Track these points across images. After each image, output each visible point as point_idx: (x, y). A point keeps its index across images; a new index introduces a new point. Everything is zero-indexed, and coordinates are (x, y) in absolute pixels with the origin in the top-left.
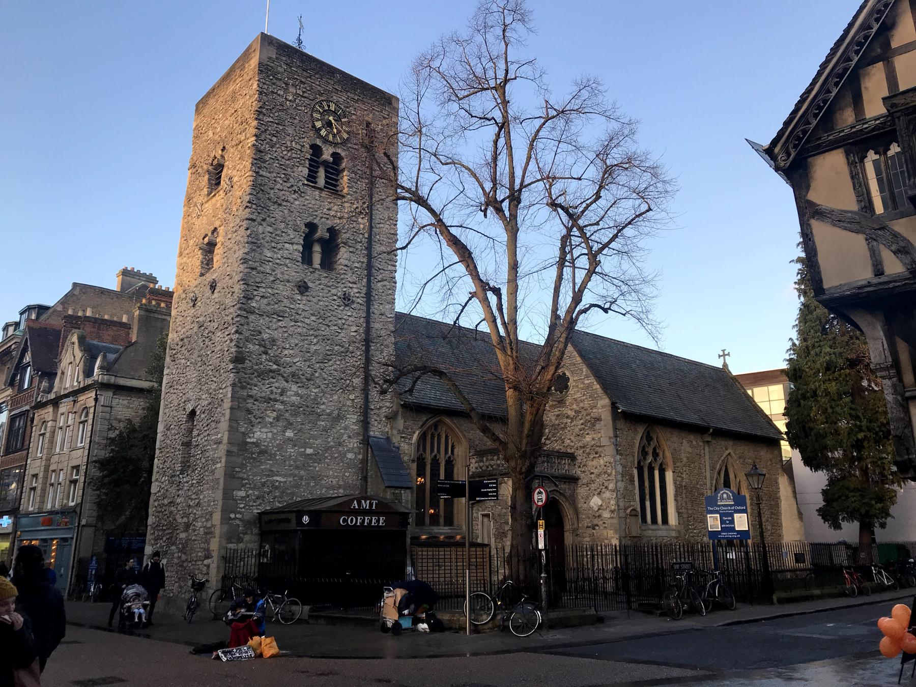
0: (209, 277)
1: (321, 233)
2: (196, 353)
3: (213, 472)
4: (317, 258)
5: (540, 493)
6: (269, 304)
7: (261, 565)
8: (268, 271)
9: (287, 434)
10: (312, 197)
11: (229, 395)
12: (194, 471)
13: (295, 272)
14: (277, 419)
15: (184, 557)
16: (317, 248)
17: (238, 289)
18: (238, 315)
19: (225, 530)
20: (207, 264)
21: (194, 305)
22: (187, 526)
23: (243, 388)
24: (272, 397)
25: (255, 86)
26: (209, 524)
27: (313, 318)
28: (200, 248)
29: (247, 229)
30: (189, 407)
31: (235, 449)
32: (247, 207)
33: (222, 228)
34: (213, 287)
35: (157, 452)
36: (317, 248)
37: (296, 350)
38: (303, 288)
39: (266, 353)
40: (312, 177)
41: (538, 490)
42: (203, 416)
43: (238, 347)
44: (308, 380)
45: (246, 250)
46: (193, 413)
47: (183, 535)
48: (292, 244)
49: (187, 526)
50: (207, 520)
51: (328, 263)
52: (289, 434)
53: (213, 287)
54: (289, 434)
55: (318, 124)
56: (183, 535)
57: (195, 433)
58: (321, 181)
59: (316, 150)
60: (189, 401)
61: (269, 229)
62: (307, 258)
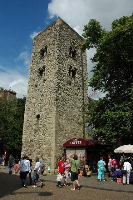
0: (42, 79)
4: (71, 75)
6: (62, 86)
8: (62, 76)
13: (68, 78)
18: (56, 87)
19: (56, 148)
26: (49, 147)
27: (72, 91)
28: (38, 72)
29: (57, 65)
30: (37, 114)
31: (57, 125)
32: (57, 59)
34: (44, 81)
35: (24, 127)
37: (69, 99)
38: (70, 83)
39: (63, 99)
40: (70, 54)
42: (43, 116)
43: (56, 96)
45: (58, 70)
46: (38, 116)
48: (67, 70)
51: (74, 76)
54: (68, 122)
55: (72, 42)
60: (37, 112)
61: (62, 65)
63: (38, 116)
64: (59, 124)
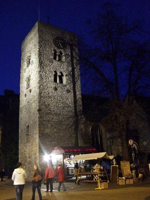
0: (29, 89)
1: (59, 74)
2: (28, 110)
3: (35, 142)
5: (131, 141)
7: (57, 168)
9: (55, 130)
10: (55, 63)
11: (38, 120)
12: (30, 142)
13: (53, 85)
14: (51, 126)
15: (29, 166)
16: (58, 78)
17: (38, 91)
20: (28, 85)
21: (26, 97)
22: (30, 157)
23: (41, 118)
24: (50, 120)
25: (38, 35)
30: (27, 125)
31: (41, 135)
33: (32, 75)
36: (58, 78)
40: (55, 58)
41: (130, 140)
44: (59, 115)
46: (28, 126)
47: (29, 160)
49: (30, 157)
50: (35, 155)
52: (55, 130)
53: (30, 91)
56: (29, 160)
57: (29, 132)
58: (57, 59)
59: (55, 52)
62: (55, 80)
63: (28, 126)
64: (43, 133)
